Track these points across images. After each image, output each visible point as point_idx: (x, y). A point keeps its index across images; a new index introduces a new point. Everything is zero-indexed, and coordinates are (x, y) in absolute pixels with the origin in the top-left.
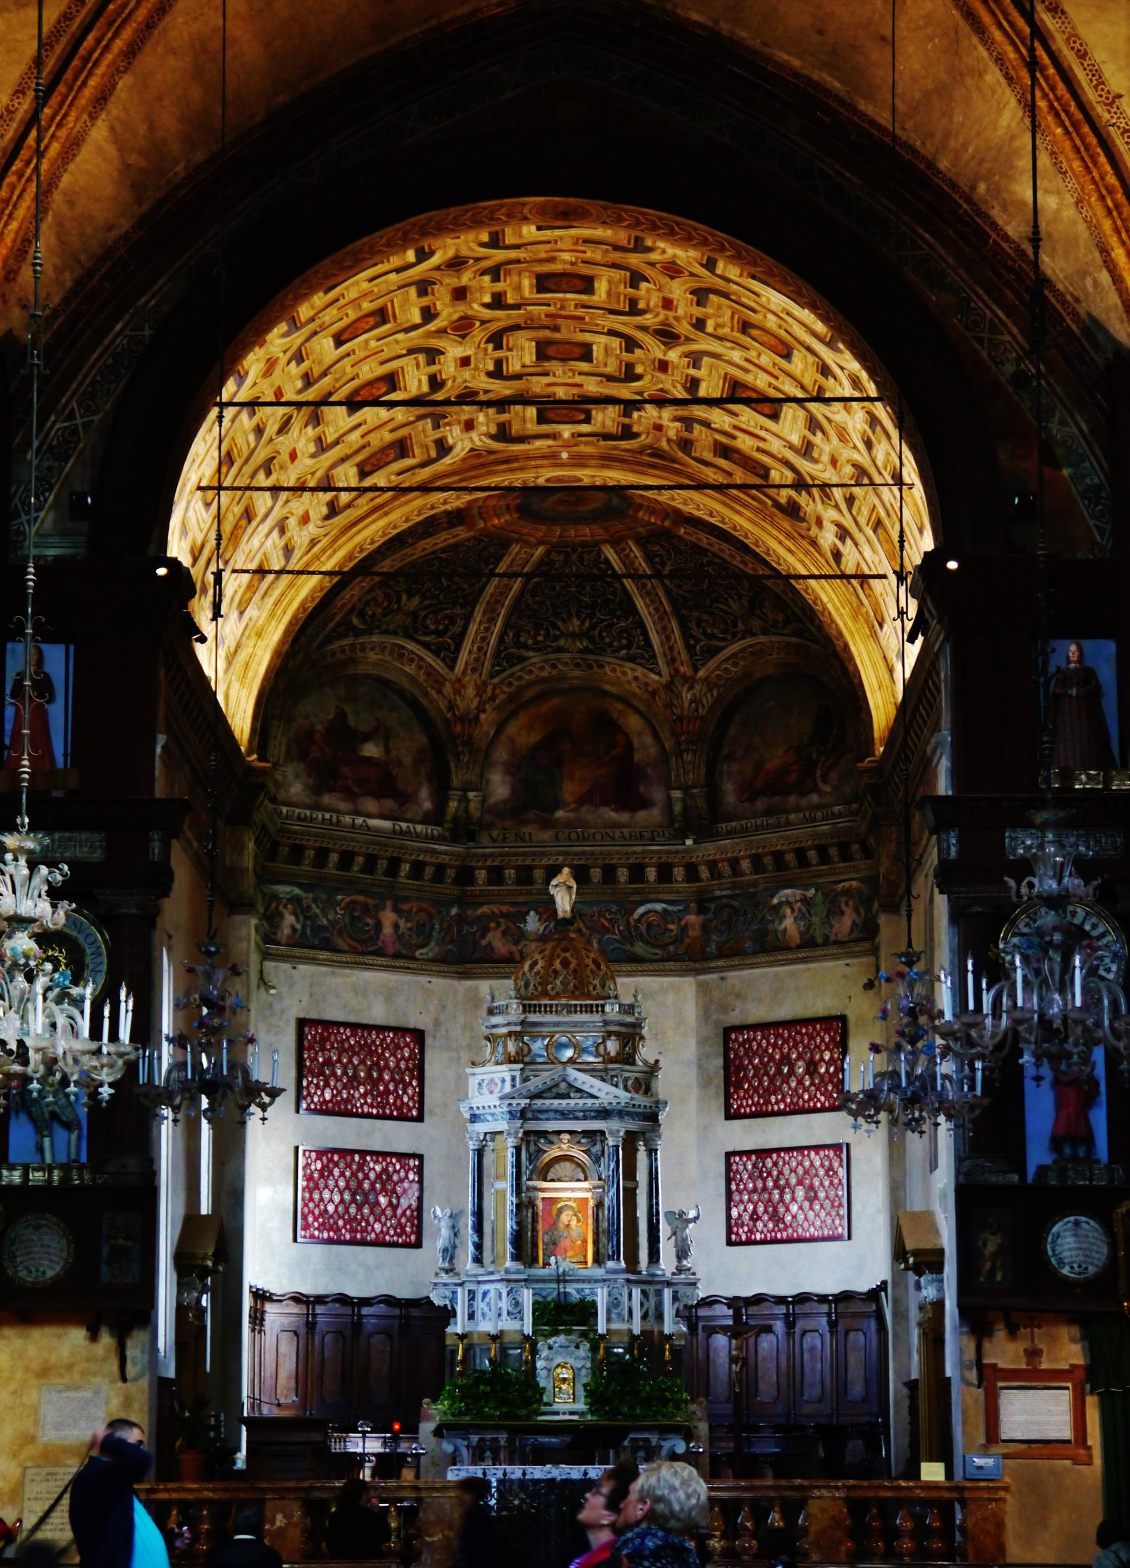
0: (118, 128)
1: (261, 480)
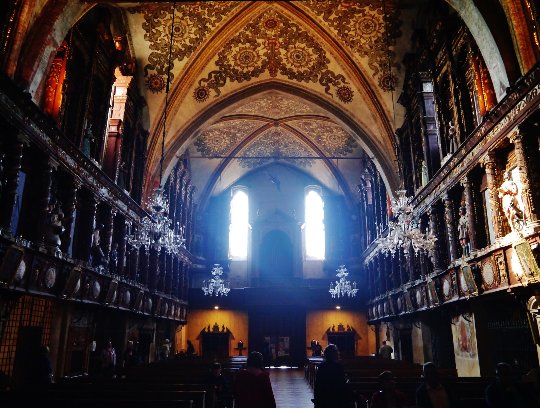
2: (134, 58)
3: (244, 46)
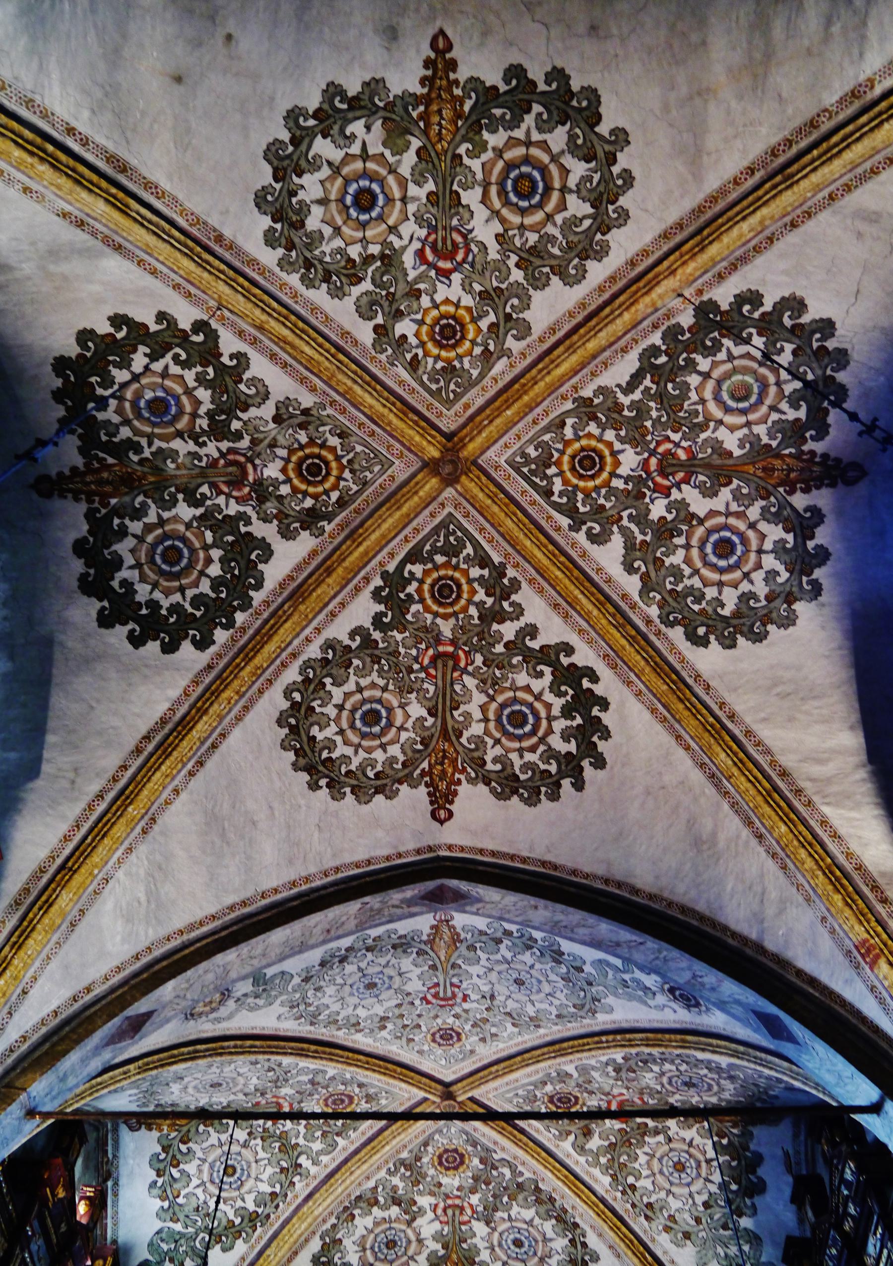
0: (856, 51)
2: (115, 1242)
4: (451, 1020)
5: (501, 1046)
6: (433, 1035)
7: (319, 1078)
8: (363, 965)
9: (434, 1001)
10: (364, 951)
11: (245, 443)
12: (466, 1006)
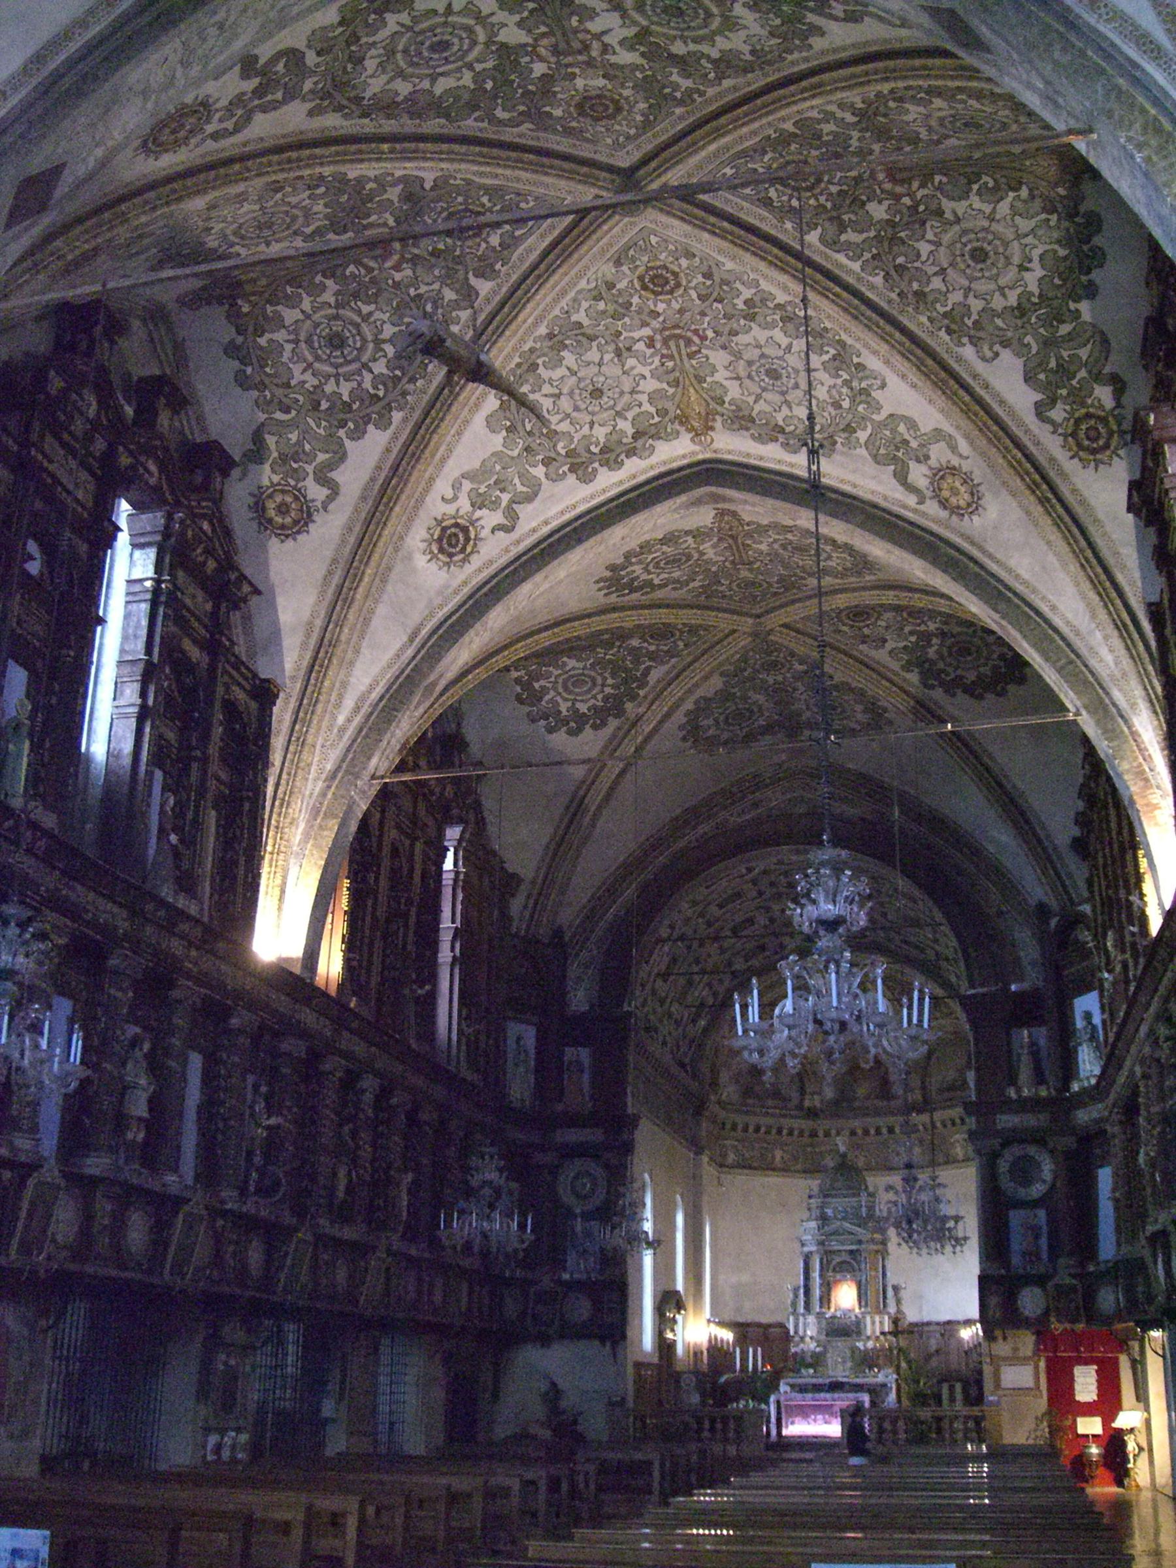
1: (696, 969)
3: (692, 47)
4: (661, 307)
5: (583, 284)
6: (678, 285)
7: (832, 229)
8: (785, 411)
9: (689, 334)
10: (788, 429)
11: (907, 629)
12: (647, 332)
